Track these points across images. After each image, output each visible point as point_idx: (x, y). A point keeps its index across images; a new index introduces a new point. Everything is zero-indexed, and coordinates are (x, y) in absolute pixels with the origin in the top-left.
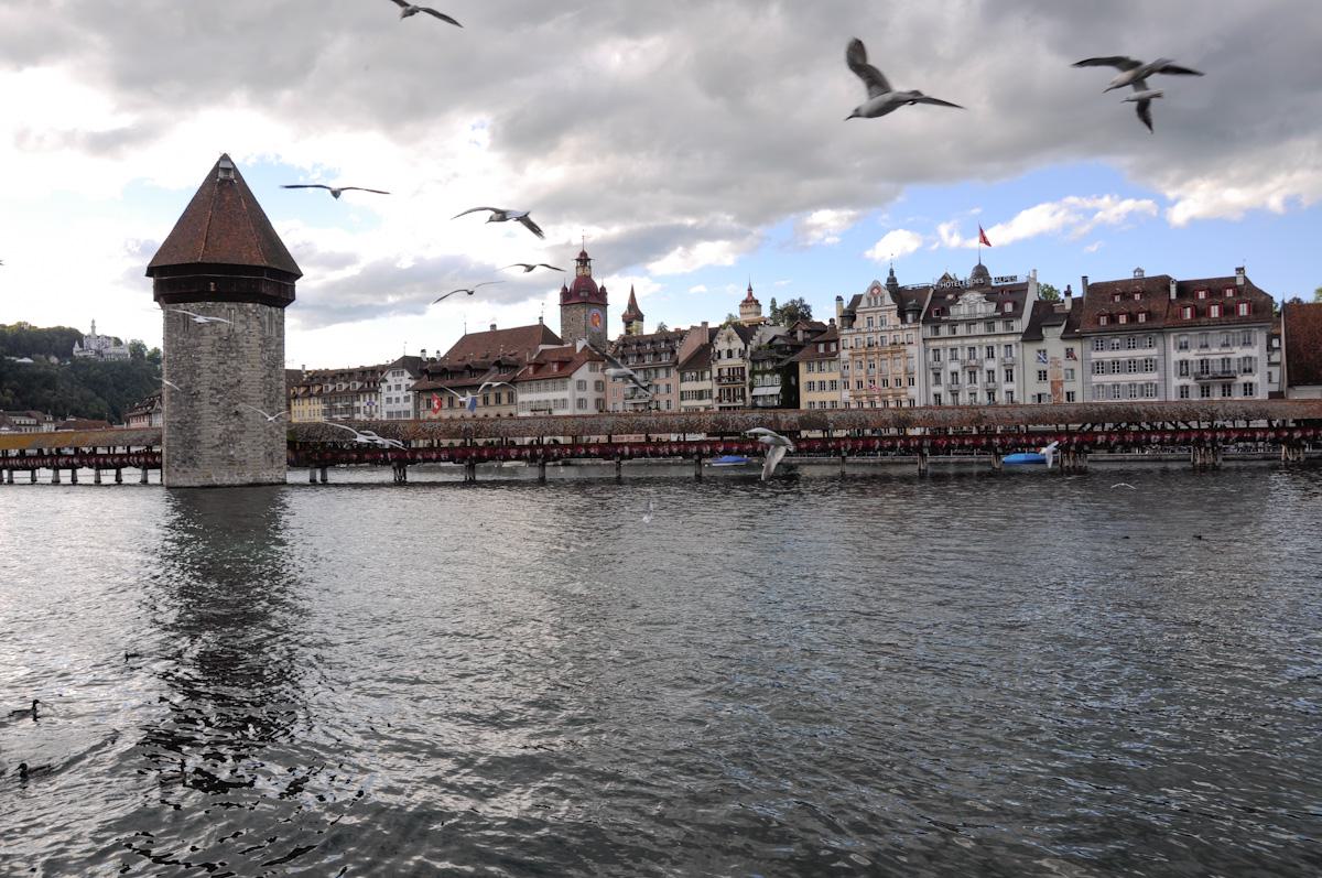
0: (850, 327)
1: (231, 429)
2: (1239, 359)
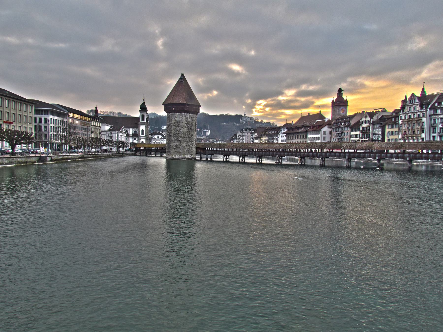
0: (403, 111)
1: (178, 144)
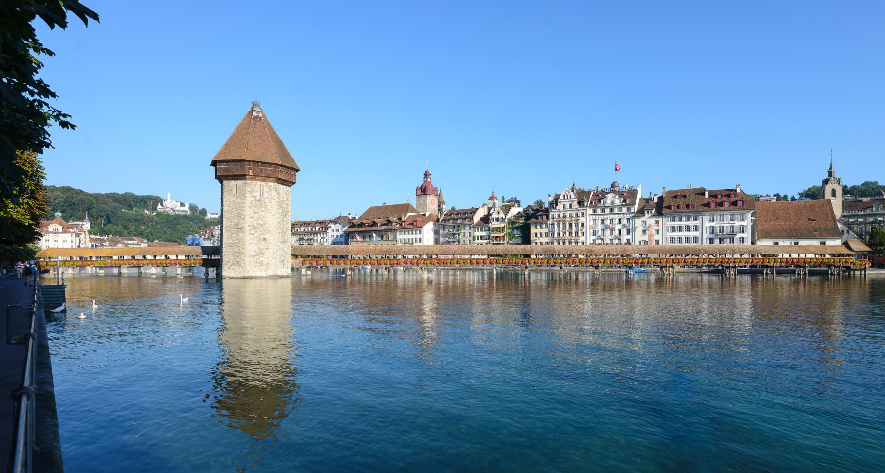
2: (738, 226)
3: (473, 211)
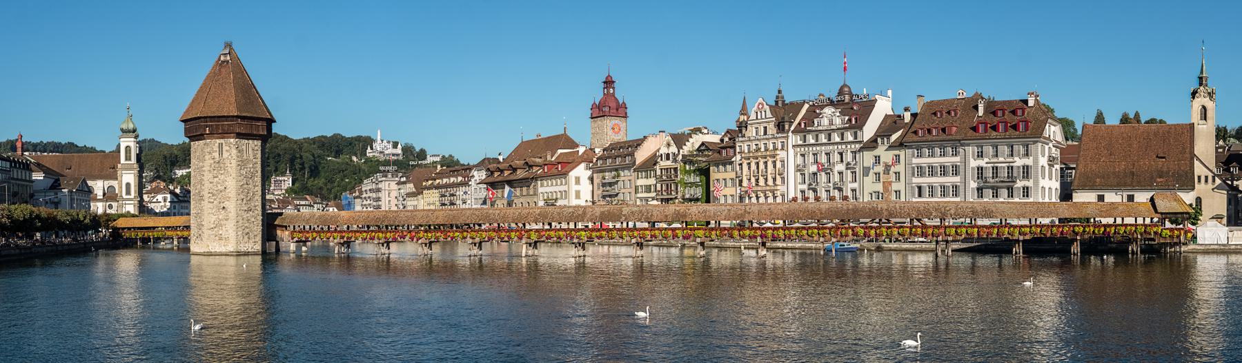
3: (638, 143)
